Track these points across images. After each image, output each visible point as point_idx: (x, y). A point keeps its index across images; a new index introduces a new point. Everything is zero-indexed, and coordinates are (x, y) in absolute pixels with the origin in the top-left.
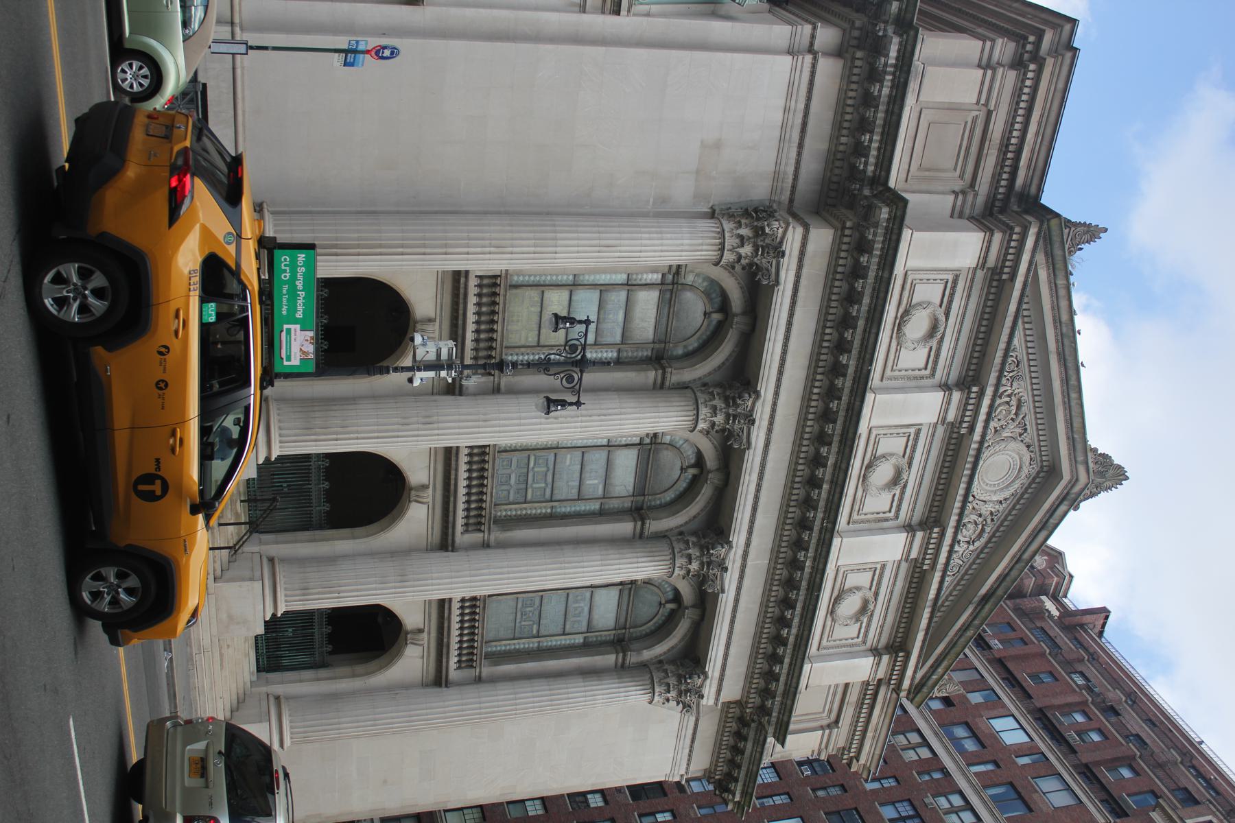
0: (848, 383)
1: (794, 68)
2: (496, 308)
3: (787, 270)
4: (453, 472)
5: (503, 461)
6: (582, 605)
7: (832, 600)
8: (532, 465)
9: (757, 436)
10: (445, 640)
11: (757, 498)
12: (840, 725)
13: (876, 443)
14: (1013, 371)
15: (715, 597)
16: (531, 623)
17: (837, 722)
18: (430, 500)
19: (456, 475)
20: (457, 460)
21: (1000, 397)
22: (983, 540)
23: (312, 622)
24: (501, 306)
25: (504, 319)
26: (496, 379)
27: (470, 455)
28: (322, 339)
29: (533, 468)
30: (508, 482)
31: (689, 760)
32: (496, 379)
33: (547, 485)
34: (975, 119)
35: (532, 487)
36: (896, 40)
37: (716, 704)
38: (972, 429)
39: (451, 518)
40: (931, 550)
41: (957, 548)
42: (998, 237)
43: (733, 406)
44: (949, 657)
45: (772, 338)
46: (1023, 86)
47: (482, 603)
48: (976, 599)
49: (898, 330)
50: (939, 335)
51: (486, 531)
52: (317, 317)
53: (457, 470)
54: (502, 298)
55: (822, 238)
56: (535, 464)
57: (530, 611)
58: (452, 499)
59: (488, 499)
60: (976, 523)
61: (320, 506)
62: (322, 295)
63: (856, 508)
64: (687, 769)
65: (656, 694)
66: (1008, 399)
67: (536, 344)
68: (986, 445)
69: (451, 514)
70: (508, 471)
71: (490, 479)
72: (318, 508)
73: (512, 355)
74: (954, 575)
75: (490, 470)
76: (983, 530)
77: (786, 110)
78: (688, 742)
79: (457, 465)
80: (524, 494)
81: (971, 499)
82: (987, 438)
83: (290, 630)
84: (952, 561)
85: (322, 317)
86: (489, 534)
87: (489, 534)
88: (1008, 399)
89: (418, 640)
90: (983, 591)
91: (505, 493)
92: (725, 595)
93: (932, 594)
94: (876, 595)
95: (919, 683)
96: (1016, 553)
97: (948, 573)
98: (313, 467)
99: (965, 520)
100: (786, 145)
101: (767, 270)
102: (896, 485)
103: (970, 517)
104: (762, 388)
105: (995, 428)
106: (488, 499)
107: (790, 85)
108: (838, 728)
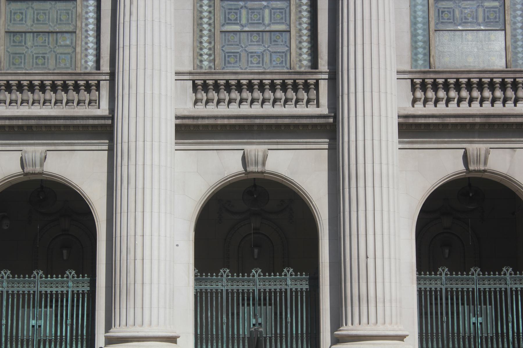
2: (70, 83)
4: (219, 122)
5: (229, 63)
8: (237, 28)
10: (478, 120)
16: (480, 10)
18: (483, 147)
19: (223, 117)
20: (203, 118)
23: (206, 293)
24: (9, 78)
25: (25, 73)
26: (103, 78)
27: (426, 101)
28: (62, 277)
29: (242, 26)
30: (261, 56)
32: (103, 78)
33: (265, 7)
35: (269, 25)
39: (287, 121)
47: (428, 76)
52: (417, 281)
53: (216, 117)
56: (237, 24)
57: (462, 12)
58: (258, 121)
59: (268, 77)
61: (286, 280)
62: (8, 277)
67: (503, 32)
69: (280, 121)
70: (244, 55)
71: (240, 77)
72: (289, 282)
73: (86, 62)
75: (227, 77)
79: (208, 117)
80: (278, 34)
83: (473, 320)
85: (67, 277)
86: (321, 73)
87: (321, 73)
89: (474, 159)
91: (274, 57)
98: (230, 288)
106: (268, 77)
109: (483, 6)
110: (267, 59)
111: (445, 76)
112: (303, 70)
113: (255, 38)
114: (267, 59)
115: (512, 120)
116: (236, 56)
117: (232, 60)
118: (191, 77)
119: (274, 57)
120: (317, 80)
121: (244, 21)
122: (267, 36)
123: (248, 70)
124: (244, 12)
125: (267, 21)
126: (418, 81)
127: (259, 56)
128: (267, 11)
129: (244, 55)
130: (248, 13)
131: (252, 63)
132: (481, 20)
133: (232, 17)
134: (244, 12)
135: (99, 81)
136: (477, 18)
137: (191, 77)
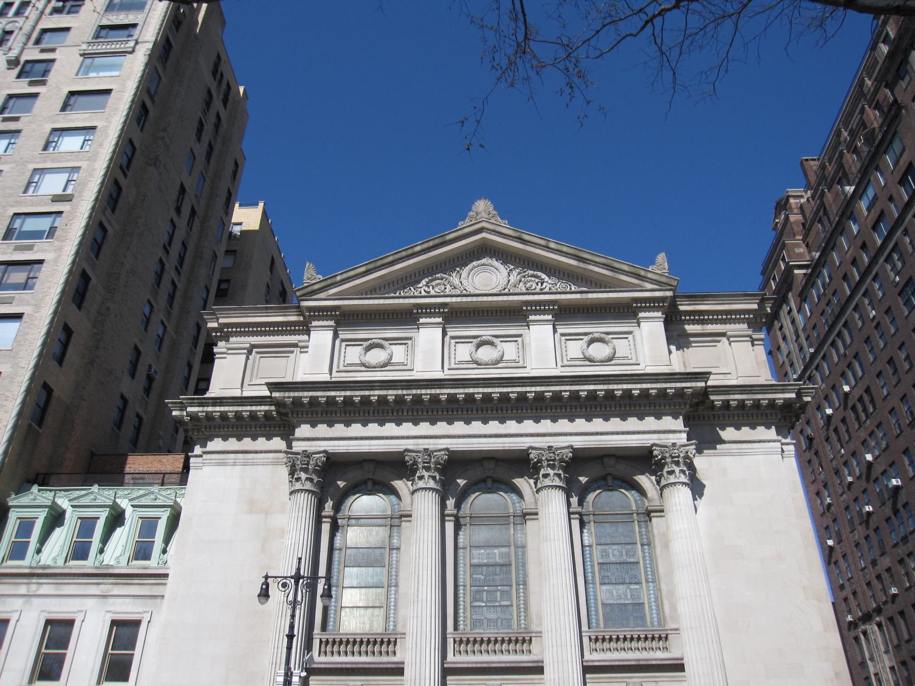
0: (390, 392)
1: (210, 464)
3: (320, 447)
5: (476, 626)
6: (611, 551)
7: (592, 364)
9: (441, 444)
11: (490, 436)
12: (725, 331)
13: (461, 362)
14: (410, 289)
15: (575, 451)
16: (628, 591)
17: (723, 335)
19: (473, 663)
20: (460, 663)
21: (429, 292)
22: (539, 274)
31: (764, 441)
34: (258, 353)
35: (500, 601)
36: (189, 409)
37: (684, 432)
38: (444, 305)
40: (540, 307)
41: (547, 290)
42: (314, 323)
43: (417, 465)
44: (637, 273)
45: (367, 447)
46: (236, 332)
48: (582, 265)
49: (375, 367)
50: (380, 341)
51: (530, 635)
54: (336, 637)
55: (304, 430)
57: (617, 592)
60: (525, 283)
63: (513, 365)
64: (774, 441)
65: (677, 481)
66: (431, 287)
68: (465, 292)
70: (485, 621)
71: (483, 636)
74: (570, 285)
76: (533, 276)
77: (234, 464)
78: (744, 446)
80: (506, 608)
81: (506, 291)
82: (459, 293)
84: (559, 290)
88: (431, 287)
90: (573, 262)
92: (573, 444)
93: (578, 296)
94: (586, 334)
95: (660, 285)
96: (542, 249)
97: (568, 290)
99: (524, 290)
100: (256, 461)
101: (317, 460)
102: (493, 343)
103: (522, 288)
104: (401, 448)
105: (452, 289)
107: (219, 464)
108: (726, 332)
109: (629, 588)
110: (499, 623)
111: (610, 634)
112: (521, 631)
113: (492, 609)
114: (499, 623)
115: (654, 662)
116: (480, 622)
117: (478, 624)
118: (453, 636)
119: (504, 622)
120: (531, 638)
121: (485, 599)
122: (499, 609)
123: (488, 631)
124: (485, 594)
125: (499, 599)
126: (593, 637)
127: (494, 622)
128: (498, 594)
129: (485, 621)
130: (487, 594)
131: (490, 626)
132: (629, 597)
133: (478, 597)
134: (485, 594)
135: (396, 639)
136: (627, 596)
137: (453, 636)
